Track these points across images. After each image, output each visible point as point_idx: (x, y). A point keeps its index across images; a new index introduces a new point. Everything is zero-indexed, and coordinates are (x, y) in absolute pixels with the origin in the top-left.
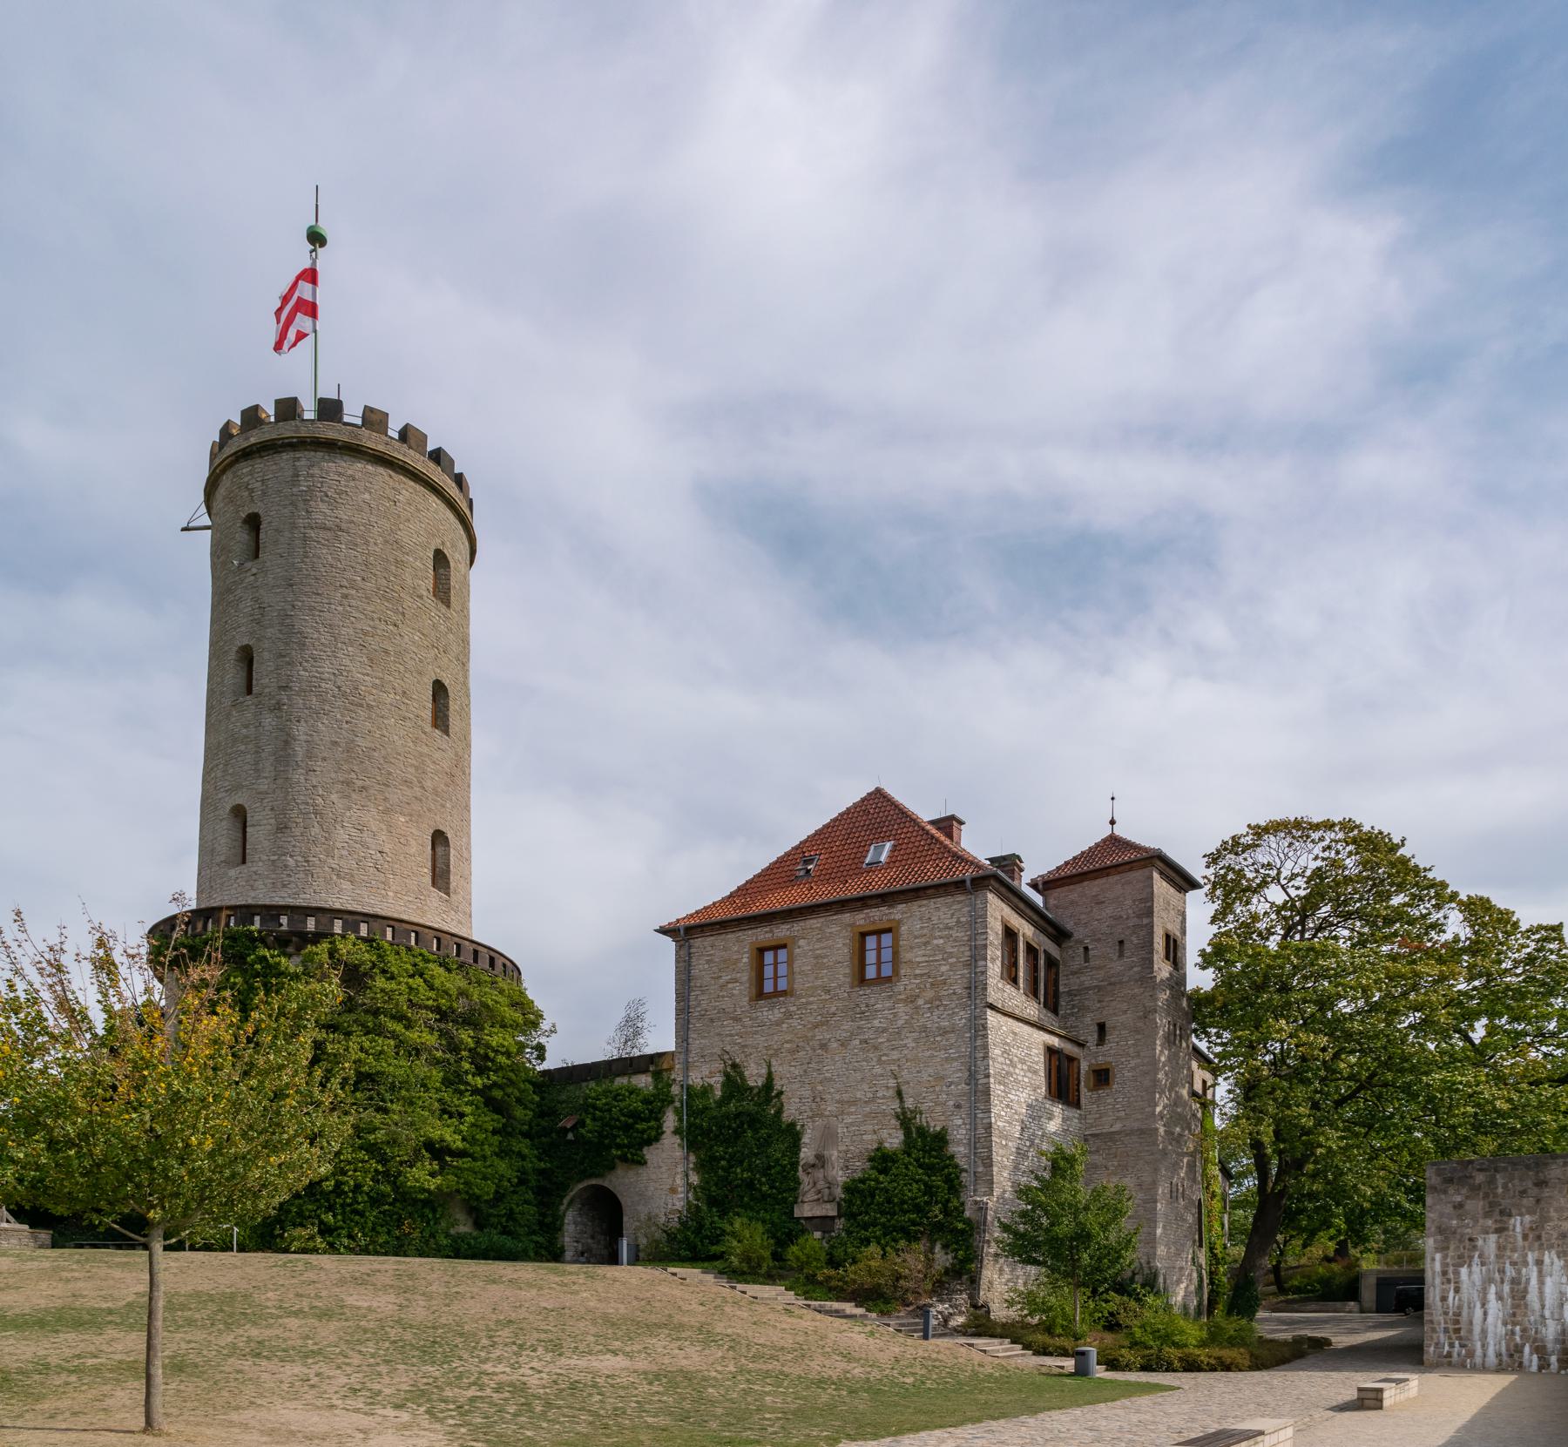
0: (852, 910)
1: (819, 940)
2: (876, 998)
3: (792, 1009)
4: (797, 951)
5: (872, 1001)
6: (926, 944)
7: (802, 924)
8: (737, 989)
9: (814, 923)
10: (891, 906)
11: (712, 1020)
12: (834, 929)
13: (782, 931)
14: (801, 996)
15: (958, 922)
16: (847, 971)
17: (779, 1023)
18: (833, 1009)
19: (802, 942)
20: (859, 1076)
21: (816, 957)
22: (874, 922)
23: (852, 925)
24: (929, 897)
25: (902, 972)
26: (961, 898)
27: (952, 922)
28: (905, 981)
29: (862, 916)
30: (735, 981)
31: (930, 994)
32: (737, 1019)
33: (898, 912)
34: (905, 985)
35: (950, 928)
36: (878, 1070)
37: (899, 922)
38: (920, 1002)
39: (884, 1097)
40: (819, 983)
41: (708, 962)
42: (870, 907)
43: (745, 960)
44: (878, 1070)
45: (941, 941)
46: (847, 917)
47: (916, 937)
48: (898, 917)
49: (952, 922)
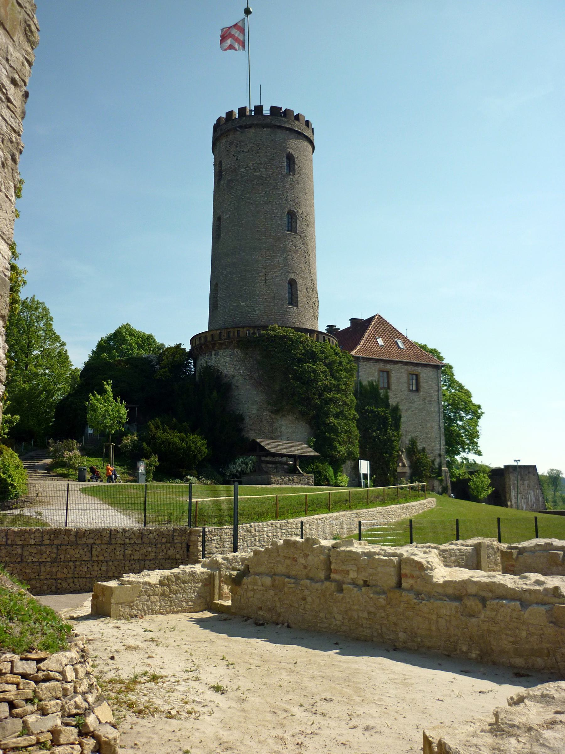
0: (408, 365)
1: (398, 373)
2: (413, 396)
6: (427, 382)
12: (403, 370)
13: (388, 367)
14: (394, 391)
20: (411, 423)
23: (408, 370)
24: (428, 367)
26: (435, 370)
28: (422, 393)
29: (410, 368)
31: (428, 399)
33: (419, 370)
34: (422, 394)
35: (433, 379)
37: (420, 373)
38: (426, 401)
39: (418, 431)
41: (365, 371)
42: (413, 366)
43: (376, 374)
44: (416, 422)
46: (406, 367)
47: (424, 379)
48: (419, 371)
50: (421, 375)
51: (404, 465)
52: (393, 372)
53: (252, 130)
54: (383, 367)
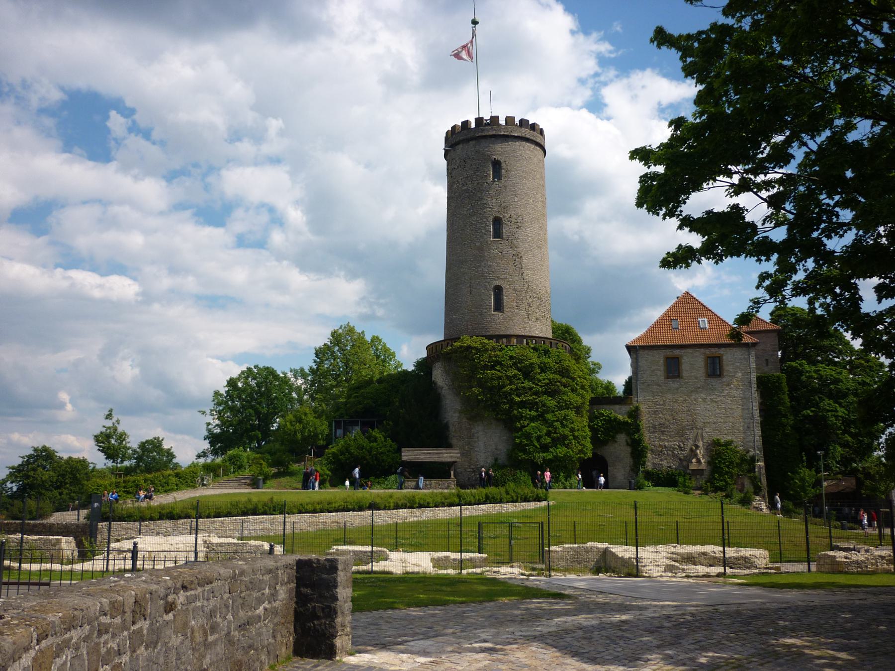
3: (682, 383)
4: (683, 361)
5: (714, 384)
6: (733, 364)
7: (685, 350)
8: (659, 373)
9: (690, 350)
10: (719, 348)
11: (648, 385)
12: (697, 354)
13: (677, 352)
14: (685, 379)
15: (744, 358)
16: (704, 371)
17: (677, 389)
18: (699, 386)
19: (685, 357)
21: (691, 364)
22: (713, 354)
23: (705, 354)
25: (725, 374)
27: (742, 357)
28: (726, 378)
30: (657, 370)
32: (659, 386)
33: (722, 351)
36: (718, 411)
37: (722, 355)
40: (693, 374)
41: (646, 361)
45: (738, 364)
48: (722, 353)
49: (742, 357)
50: (724, 357)
51: (699, 461)
52: (685, 357)
53: (461, 146)
54: (671, 353)
